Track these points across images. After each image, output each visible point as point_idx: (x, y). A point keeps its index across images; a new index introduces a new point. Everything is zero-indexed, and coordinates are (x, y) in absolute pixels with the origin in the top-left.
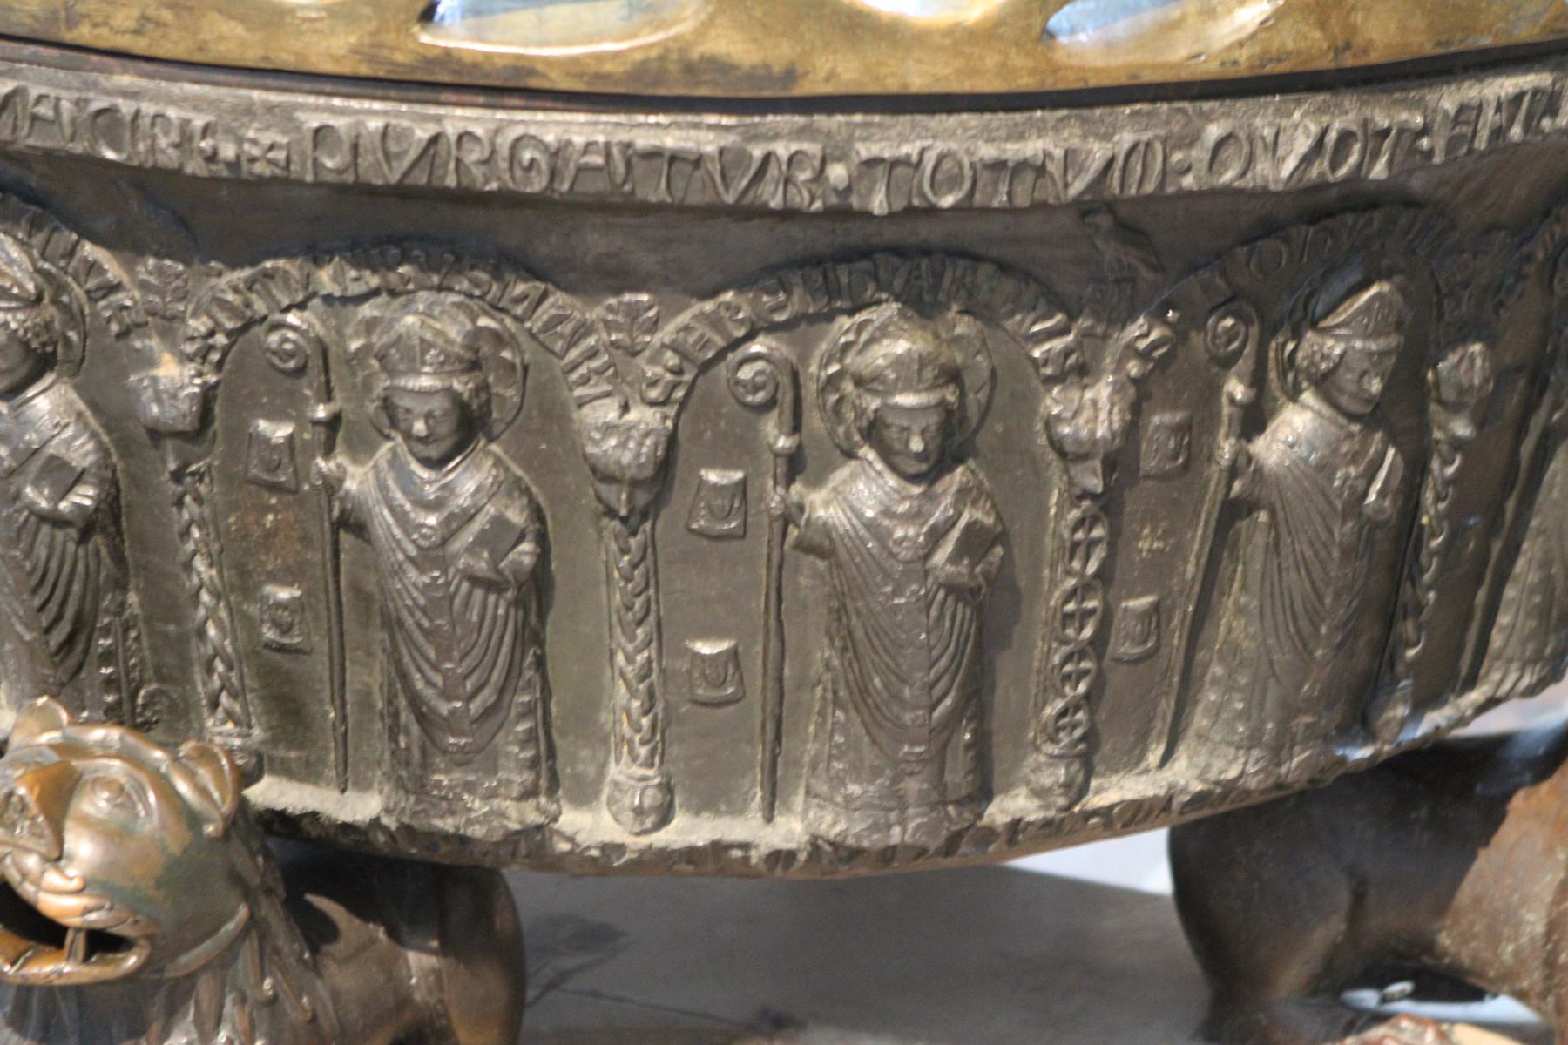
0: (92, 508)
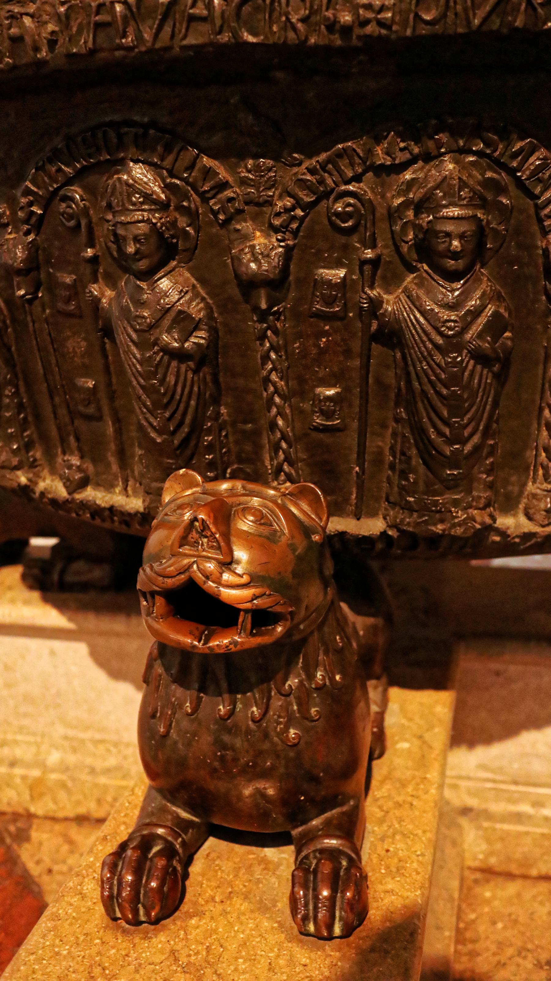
0: (205, 345)
